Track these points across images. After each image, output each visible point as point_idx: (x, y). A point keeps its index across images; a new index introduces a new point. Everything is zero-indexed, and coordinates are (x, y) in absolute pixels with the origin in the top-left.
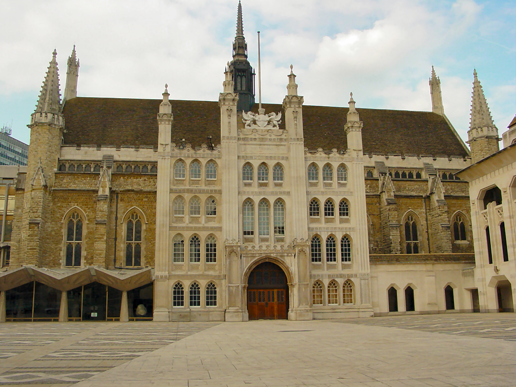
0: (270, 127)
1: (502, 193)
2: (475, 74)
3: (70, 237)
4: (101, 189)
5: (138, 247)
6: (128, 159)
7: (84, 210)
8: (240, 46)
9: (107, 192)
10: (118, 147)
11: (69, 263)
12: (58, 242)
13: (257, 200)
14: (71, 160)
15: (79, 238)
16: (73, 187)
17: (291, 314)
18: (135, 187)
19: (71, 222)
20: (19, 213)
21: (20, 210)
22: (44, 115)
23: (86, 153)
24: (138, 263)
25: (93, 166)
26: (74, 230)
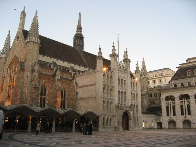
0: (123, 68)
1: (175, 98)
2: (143, 59)
3: (41, 94)
4: (57, 76)
5: (64, 101)
6: (60, 65)
7: (48, 84)
8: (79, 28)
9: (59, 78)
10: (57, 60)
11: (41, 106)
12: (38, 95)
13: (121, 91)
14: (41, 61)
15: (45, 95)
16: (44, 73)
17: (131, 129)
18: (65, 77)
19: (42, 88)
20: (21, 81)
21: (22, 79)
22: (36, 39)
23: (46, 59)
24: (64, 107)
25: (48, 65)
26: (43, 92)
